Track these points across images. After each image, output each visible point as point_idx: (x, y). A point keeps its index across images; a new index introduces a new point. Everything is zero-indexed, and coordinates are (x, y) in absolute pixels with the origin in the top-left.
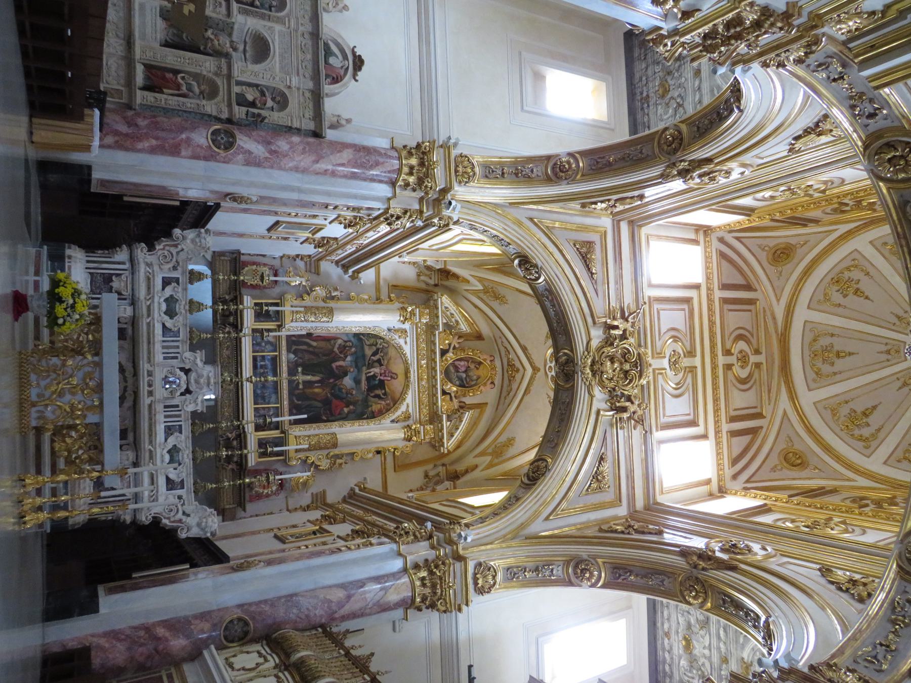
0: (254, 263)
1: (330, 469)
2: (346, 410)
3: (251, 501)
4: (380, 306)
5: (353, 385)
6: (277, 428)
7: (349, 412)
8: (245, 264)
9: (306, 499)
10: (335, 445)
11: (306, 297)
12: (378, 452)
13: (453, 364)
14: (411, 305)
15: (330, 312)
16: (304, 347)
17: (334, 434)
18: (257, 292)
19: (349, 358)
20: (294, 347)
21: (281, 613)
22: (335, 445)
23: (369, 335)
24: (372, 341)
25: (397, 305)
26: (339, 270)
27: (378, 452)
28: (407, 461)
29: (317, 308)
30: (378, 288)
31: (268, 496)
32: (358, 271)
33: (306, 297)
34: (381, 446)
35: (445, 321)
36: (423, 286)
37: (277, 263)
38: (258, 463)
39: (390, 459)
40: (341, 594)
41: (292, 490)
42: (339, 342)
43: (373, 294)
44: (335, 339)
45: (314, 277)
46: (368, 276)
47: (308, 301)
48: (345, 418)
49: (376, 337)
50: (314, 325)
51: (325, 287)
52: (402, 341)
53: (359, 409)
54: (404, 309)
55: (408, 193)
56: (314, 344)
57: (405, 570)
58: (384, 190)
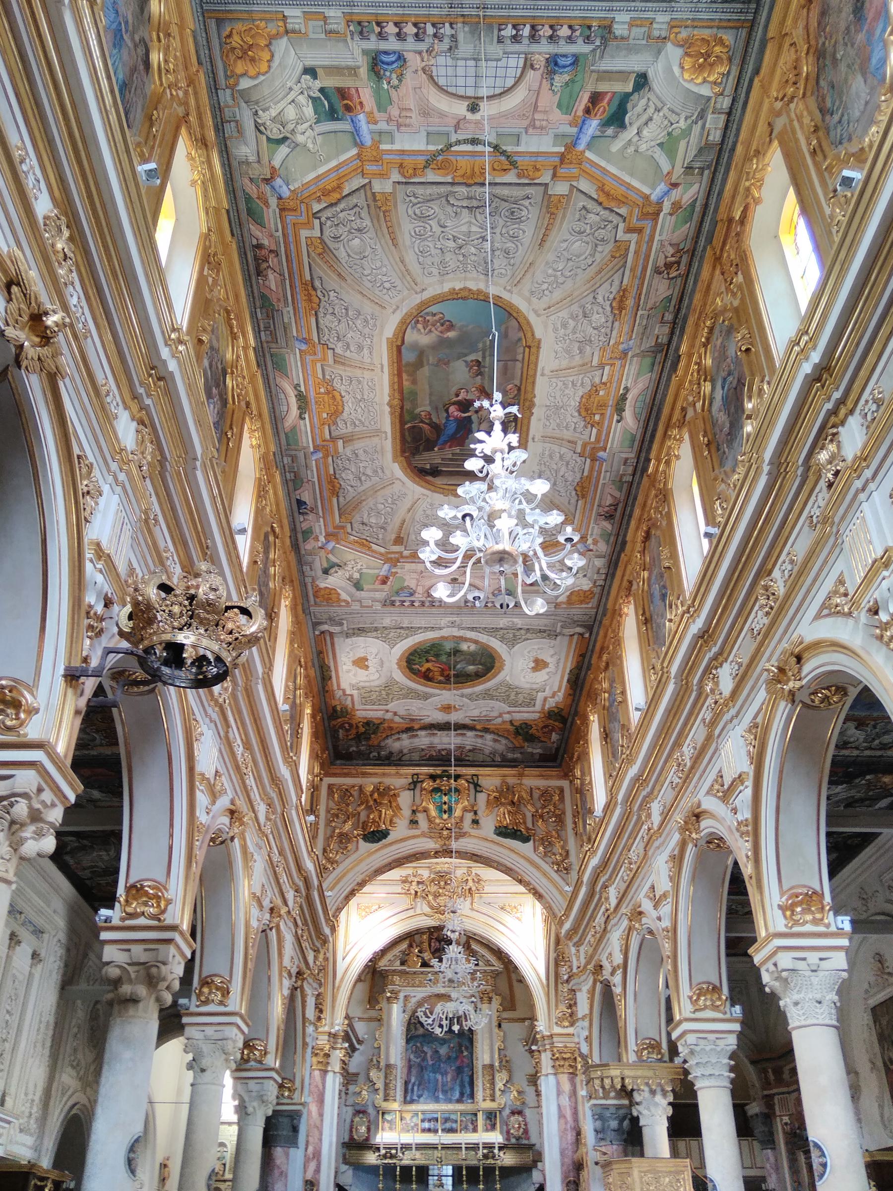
0: (351, 1131)
1: (510, 1071)
2: (465, 1053)
3: (528, 1139)
4: (384, 1017)
5: (446, 1046)
6: (476, 1115)
7: (467, 1048)
8: (351, 1138)
9: (530, 1090)
10: (492, 1066)
11: (376, 1087)
12: (500, 1026)
13: (433, 953)
14: (384, 991)
15: (388, 1066)
16: (416, 1088)
17: (484, 1066)
18: (372, 1127)
19: (425, 1049)
20: (415, 1098)
21: (568, 1161)
22: (492, 1066)
23: (408, 1030)
24: (412, 1027)
25: (383, 1004)
26: (356, 1054)
27: (500, 1026)
28: (508, 998)
29: (386, 1077)
30: (370, 1019)
31: (526, 1125)
32: (360, 1042)
33: (376, 1087)
34: (495, 1023)
35: (398, 963)
36: (369, 976)
37: (350, 1111)
38: (501, 1133)
39: (505, 1015)
40: (563, 1121)
41: (523, 1103)
42: (412, 1057)
43: (376, 1023)
44: (410, 1061)
45: (361, 1079)
46: (361, 1028)
47: (380, 1085)
48: (472, 1054)
49: (409, 1023)
50: (399, 1080)
51: (369, 1069)
52: (414, 1000)
53: (466, 1043)
54: (388, 998)
55: (331, 1060)
56: (413, 1080)
57: (555, 1074)
58: (330, 1077)
